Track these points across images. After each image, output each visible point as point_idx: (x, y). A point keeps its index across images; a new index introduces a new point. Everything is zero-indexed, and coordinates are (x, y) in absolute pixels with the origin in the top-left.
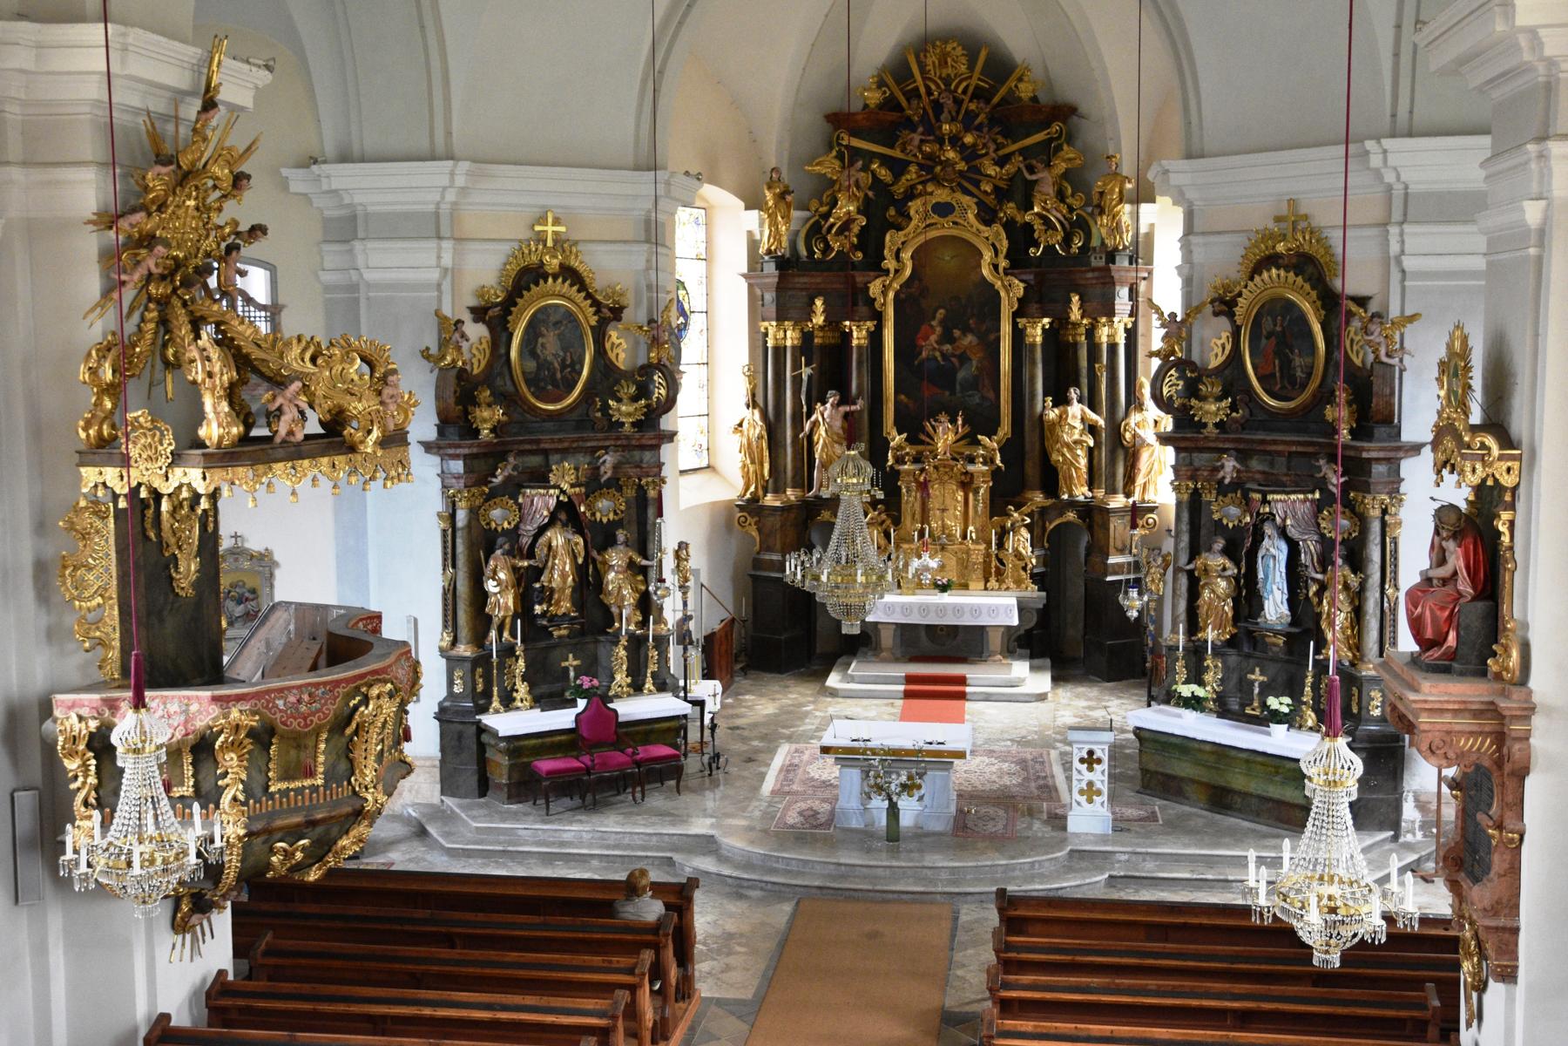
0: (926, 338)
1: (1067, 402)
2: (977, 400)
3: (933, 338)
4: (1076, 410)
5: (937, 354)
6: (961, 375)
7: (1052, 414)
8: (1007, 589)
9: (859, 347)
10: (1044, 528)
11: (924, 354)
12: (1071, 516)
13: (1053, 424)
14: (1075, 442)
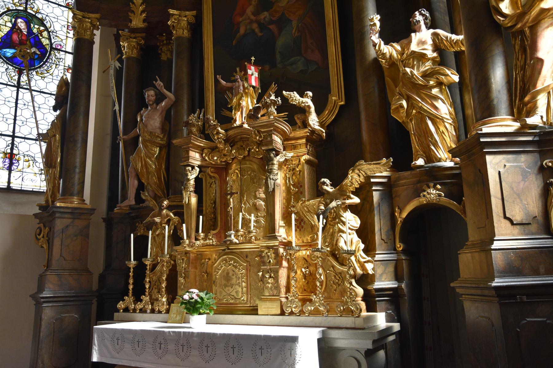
0: (243, 13)
1: (412, 28)
2: (300, 66)
3: (249, 10)
4: (422, 39)
5: (255, 26)
6: (281, 42)
7: (390, 50)
8: (316, 312)
9: (179, 38)
10: (393, 219)
11: (242, 31)
12: (433, 194)
13: (392, 63)
14: (426, 75)
